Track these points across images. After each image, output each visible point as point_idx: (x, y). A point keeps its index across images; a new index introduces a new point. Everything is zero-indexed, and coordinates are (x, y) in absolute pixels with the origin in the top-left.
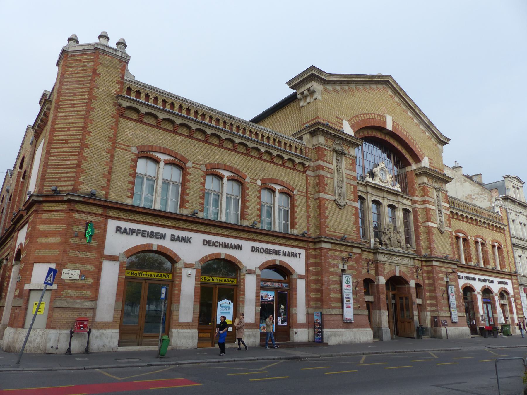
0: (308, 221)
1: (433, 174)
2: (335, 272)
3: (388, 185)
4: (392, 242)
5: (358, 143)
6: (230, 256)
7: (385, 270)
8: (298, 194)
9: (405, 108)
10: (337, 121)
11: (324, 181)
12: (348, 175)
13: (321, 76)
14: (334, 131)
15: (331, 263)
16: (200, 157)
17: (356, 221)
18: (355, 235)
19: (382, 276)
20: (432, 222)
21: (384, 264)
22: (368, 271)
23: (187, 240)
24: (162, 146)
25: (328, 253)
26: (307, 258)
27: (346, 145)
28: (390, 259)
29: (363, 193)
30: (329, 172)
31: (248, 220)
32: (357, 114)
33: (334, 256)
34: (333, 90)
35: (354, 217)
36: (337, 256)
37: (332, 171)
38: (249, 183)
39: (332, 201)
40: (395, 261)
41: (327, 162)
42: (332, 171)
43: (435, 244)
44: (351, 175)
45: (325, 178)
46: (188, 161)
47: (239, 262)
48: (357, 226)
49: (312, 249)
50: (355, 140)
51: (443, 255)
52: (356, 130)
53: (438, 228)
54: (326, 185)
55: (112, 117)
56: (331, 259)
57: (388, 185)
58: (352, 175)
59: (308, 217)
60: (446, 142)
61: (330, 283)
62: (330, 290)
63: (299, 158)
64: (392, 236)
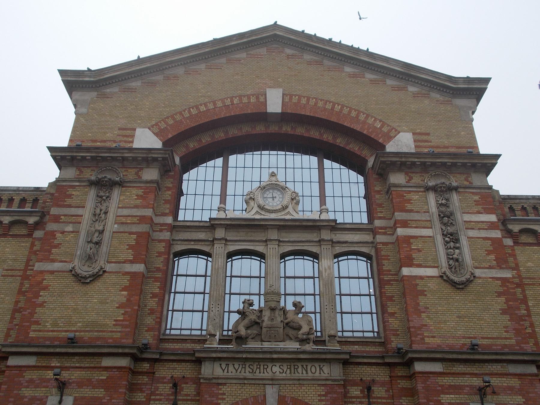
1: (416, 160)
3: (289, 213)
4: (264, 330)
5: (156, 156)
7: (224, 399)
9: (335, 64)
10: (118, 135)
12: (129, 216)
14: (88, 152)
17: (128, 300)
18: (119, 330)
21: (225, 384)
25: (24, 377)
27: (134, 168)
28: (248, 369)
30: (70, 223)
33: (39, 379)
35: (125, 293)
37: (79, 219)
39: (67, 272)
40: (266, 375)
41: (72, 207)
42: (79, 219)
43: (428, 317)
44: (137, 216)
45: (58, 235)
48: (130, 310)
49: (402, 377)
51: (462, 341)
52: (170, 136)
53: (441, 277)
54: (57, 246)
56: (27, 387)
57: (289, 213)
58: (138, 214)
63: (12, 214)
64: (266, 319)
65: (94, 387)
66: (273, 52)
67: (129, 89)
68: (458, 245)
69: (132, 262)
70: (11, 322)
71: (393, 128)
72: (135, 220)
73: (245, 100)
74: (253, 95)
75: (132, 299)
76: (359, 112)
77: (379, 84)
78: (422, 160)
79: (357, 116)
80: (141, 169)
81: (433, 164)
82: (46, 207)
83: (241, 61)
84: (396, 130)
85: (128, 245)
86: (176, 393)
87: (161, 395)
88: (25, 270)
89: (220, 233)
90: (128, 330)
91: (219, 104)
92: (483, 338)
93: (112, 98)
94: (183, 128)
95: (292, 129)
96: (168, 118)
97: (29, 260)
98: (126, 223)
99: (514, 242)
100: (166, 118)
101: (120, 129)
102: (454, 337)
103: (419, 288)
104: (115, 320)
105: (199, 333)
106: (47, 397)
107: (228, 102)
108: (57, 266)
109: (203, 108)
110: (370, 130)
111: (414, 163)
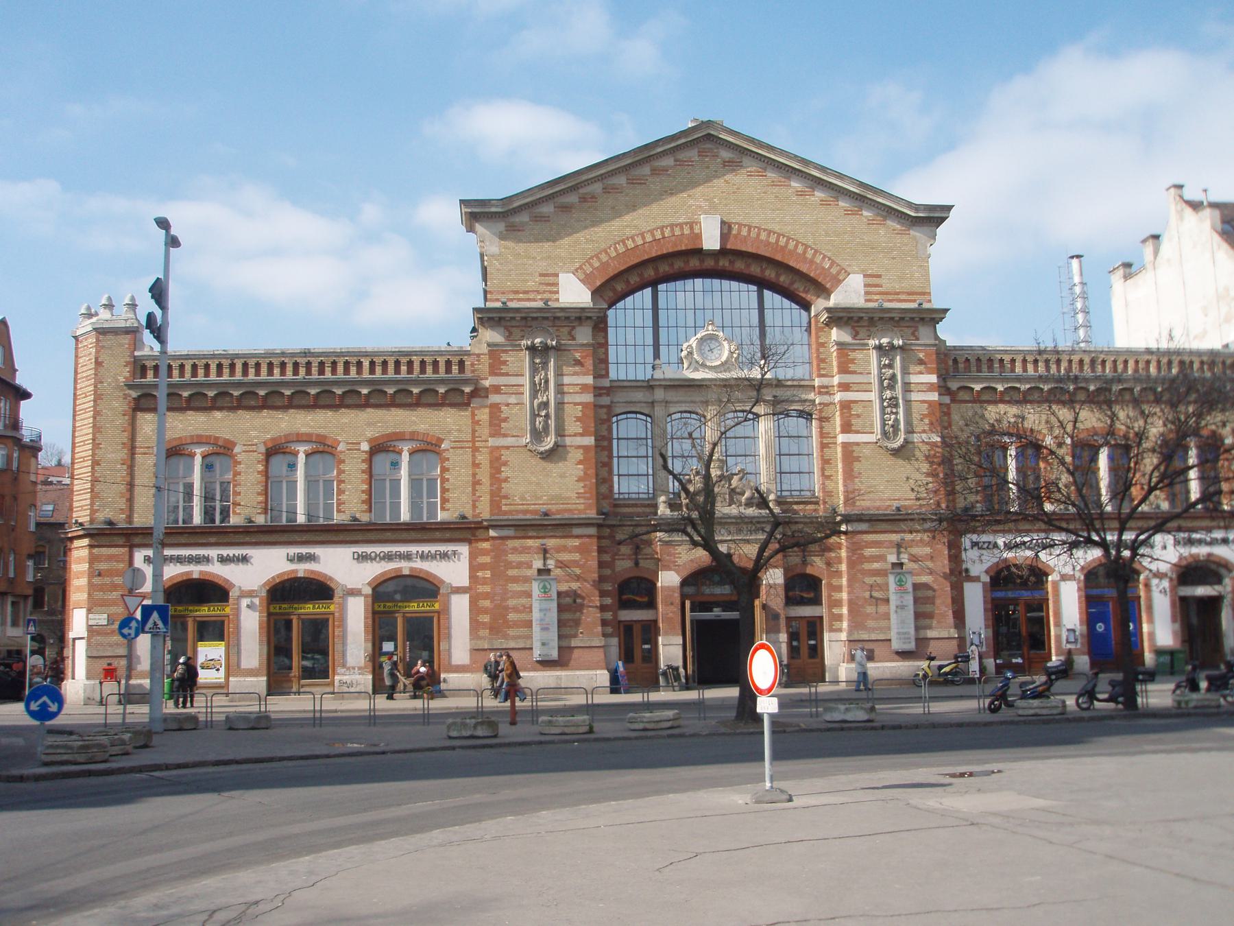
0: (474, 490)
2: (523, 577)
6: (312, 572)
8: (451, 448)
10: (540, 284)
11: (498, 414)
13: (487, 210)
15: (511, 562)
16: (253, 433)
17: (585, 473)
18: (582, 502)
19: (668, 568)
20: (857, 432)
22: (637, 564)
23: (244, 559)
24: (195, 433)
26: (472, 556)
29: (639, 405)
30: (512, 394)
31: (344, 512)
32: (603, 246)
34: (531, 221)
35: (581, 467)
36: (530, 548)
38: (344, 452)
41: (510, 375)
43: (861, 482)
44: (578, 385)
45: (503, 408)
46: (234, 444)
47: (331, 579)
48: (588, 483)
50: (581, 312)
52: (598, 283)
54: (505, 420)
55: (124, 415)
56: (512, 553)
58: (579, 382)
59: (476, 483)
60: (936, 215)
61: (509, 595)
62: (507, 608)
65: (570, 552)
66: (707, 156)
67: (541, 217)
68: (894, 410)
69: (581, 435)
70: (474, 494)
71: (843, 269)
72: (577, 389)
73: (677, 232)
74: (686, 224)
75: (589, 472)
76: (806, 247)
77: (830, 205)
78: (869, 315)
79: (805, 252)
80: (574, 328)
81: (881, 319)
82: (476, 370)
83: (667, 171)
84: (846, 272)
85: (575, 417)
86: (636, 554)
87: (624, 555)
88: (473, 441)
89: (659, 394)
90: (591, 501)
91: (649, 238)
92: (906, 500)
93: (523, 230)
94: (611, 273)
95: (730, 262)
96: (592, 258)
97: (474, 431)
98: (571, 393)
99: (951, 400)
100: (590, 259)
101: (541, 275)
102: (881, 500)
103: (855, 454)
104: (577, 493)
105: (645, 496)
106: (531, 561)
107: (658, 235)
108: (509, 441)
109: (630, 244)
110: (818, 272)
111: (861, 318)
